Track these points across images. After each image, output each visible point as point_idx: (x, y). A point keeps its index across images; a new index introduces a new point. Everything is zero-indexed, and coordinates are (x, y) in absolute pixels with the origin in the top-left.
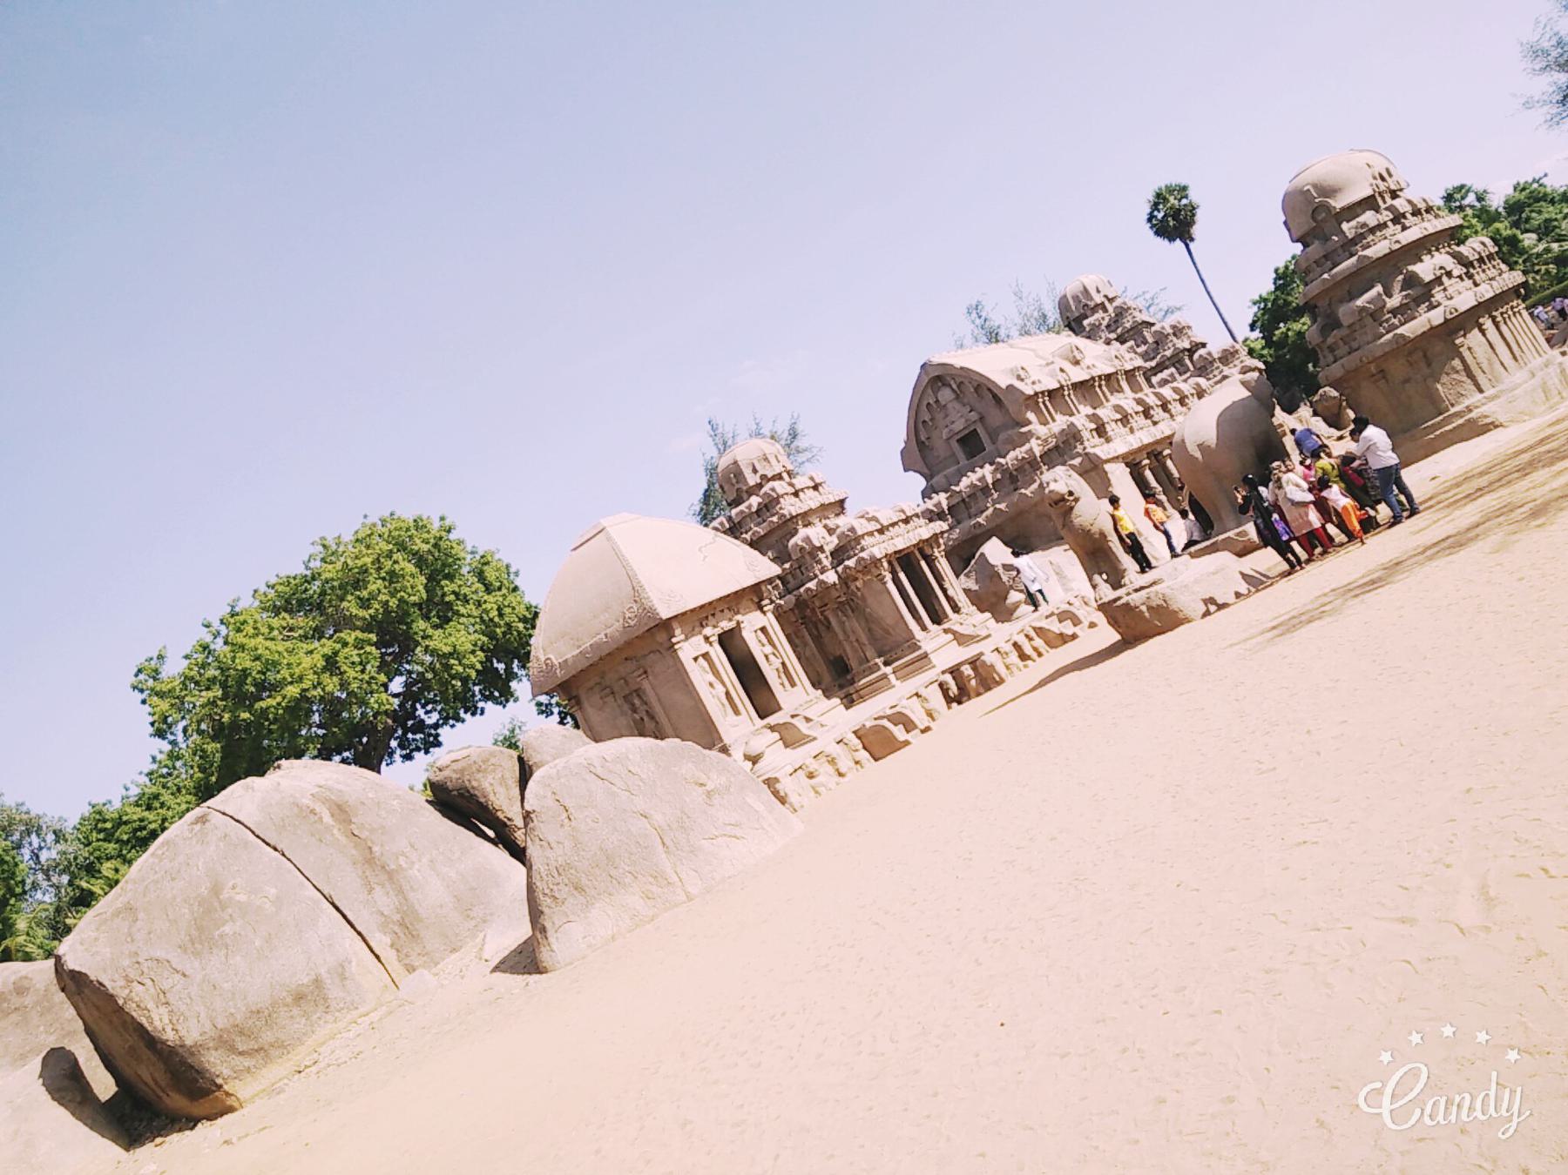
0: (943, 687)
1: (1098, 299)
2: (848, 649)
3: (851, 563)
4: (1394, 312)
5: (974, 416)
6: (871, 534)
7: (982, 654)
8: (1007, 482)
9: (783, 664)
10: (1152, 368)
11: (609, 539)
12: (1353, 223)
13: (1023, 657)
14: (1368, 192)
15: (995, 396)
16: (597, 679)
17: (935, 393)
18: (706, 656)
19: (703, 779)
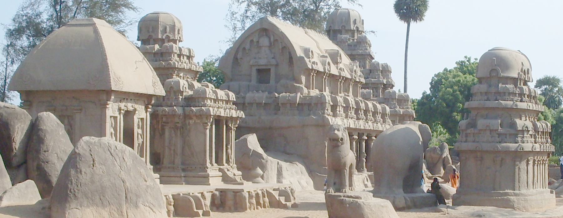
0: (213, 196)
1: (352, 27)
2: (167, 151)
4: (499, 135)
6: (211, 99)
7: (243, 190)
9: (143, 142)
13: (258, 203)
14: (516, 76)
15: (291, 58)
17: (260, 37)
18: (115, 118)
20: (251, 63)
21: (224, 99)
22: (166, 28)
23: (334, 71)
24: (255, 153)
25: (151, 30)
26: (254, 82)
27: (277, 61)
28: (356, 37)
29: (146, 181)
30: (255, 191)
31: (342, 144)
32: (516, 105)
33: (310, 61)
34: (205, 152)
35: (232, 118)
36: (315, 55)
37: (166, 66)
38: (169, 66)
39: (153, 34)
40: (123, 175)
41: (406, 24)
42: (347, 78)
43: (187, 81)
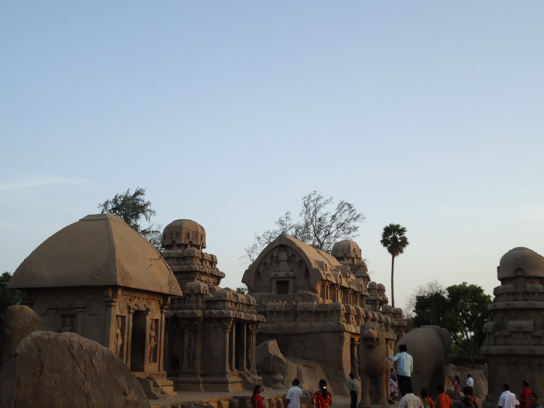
3: (214, 312)
4: (534, 337)
9: (156, 346)
12: (532, 285)
18: (123, 317)
20: (273, 274)
21: (245, 302)
22: (189, 234)
23: (345, 284)
24: (276, 358)
25: (174, 235)
26: (274, 293)
29: (126, 395)
30: (276, 399)
31: (378, 345)
33: (324, 273)
34: (224, 355)
35: (252, 322)
36: (328, 269)
37: (188, 270)
38: (190, 269)
39: (174, 239)
40: (88, 387)
41: (391, 256)
43: (209, 285)
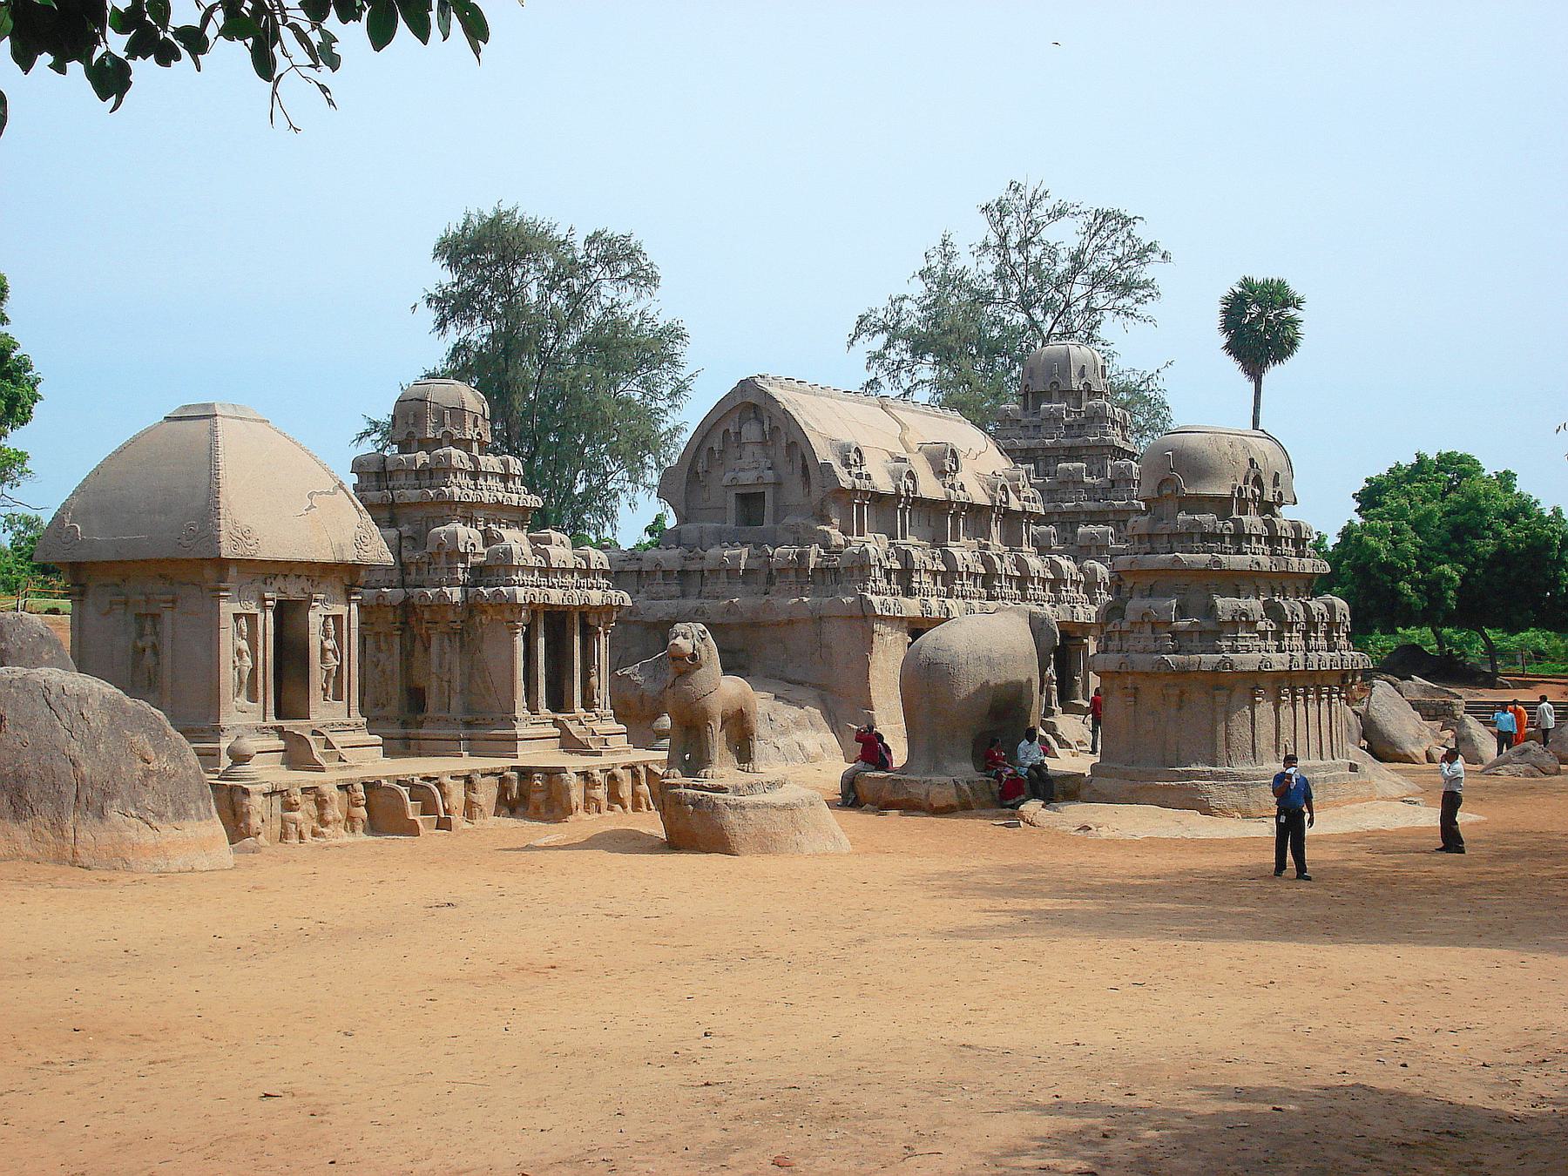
0: (504, 783)
1: (1076, 384)
4: (1175, 634)
5: (769, 476)
6: (530, 570)
7: (564, 770)
8: (762, 578)
9: (340, 668)
10: (1092, 513)
11: (213, 432)
13: (614, 797)
15: (805, 467)
16: (117, 580)
18: (252, 618)
19: (151, 755)
26: (731, 524)
27: (778, 476)
28: (1084, 405)
32: (1219, 563)
39: (413, 429)
42: (981, 507)
